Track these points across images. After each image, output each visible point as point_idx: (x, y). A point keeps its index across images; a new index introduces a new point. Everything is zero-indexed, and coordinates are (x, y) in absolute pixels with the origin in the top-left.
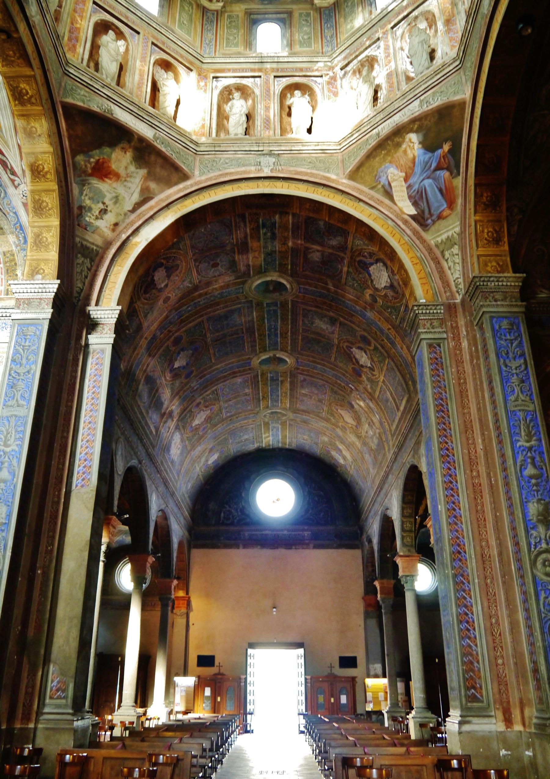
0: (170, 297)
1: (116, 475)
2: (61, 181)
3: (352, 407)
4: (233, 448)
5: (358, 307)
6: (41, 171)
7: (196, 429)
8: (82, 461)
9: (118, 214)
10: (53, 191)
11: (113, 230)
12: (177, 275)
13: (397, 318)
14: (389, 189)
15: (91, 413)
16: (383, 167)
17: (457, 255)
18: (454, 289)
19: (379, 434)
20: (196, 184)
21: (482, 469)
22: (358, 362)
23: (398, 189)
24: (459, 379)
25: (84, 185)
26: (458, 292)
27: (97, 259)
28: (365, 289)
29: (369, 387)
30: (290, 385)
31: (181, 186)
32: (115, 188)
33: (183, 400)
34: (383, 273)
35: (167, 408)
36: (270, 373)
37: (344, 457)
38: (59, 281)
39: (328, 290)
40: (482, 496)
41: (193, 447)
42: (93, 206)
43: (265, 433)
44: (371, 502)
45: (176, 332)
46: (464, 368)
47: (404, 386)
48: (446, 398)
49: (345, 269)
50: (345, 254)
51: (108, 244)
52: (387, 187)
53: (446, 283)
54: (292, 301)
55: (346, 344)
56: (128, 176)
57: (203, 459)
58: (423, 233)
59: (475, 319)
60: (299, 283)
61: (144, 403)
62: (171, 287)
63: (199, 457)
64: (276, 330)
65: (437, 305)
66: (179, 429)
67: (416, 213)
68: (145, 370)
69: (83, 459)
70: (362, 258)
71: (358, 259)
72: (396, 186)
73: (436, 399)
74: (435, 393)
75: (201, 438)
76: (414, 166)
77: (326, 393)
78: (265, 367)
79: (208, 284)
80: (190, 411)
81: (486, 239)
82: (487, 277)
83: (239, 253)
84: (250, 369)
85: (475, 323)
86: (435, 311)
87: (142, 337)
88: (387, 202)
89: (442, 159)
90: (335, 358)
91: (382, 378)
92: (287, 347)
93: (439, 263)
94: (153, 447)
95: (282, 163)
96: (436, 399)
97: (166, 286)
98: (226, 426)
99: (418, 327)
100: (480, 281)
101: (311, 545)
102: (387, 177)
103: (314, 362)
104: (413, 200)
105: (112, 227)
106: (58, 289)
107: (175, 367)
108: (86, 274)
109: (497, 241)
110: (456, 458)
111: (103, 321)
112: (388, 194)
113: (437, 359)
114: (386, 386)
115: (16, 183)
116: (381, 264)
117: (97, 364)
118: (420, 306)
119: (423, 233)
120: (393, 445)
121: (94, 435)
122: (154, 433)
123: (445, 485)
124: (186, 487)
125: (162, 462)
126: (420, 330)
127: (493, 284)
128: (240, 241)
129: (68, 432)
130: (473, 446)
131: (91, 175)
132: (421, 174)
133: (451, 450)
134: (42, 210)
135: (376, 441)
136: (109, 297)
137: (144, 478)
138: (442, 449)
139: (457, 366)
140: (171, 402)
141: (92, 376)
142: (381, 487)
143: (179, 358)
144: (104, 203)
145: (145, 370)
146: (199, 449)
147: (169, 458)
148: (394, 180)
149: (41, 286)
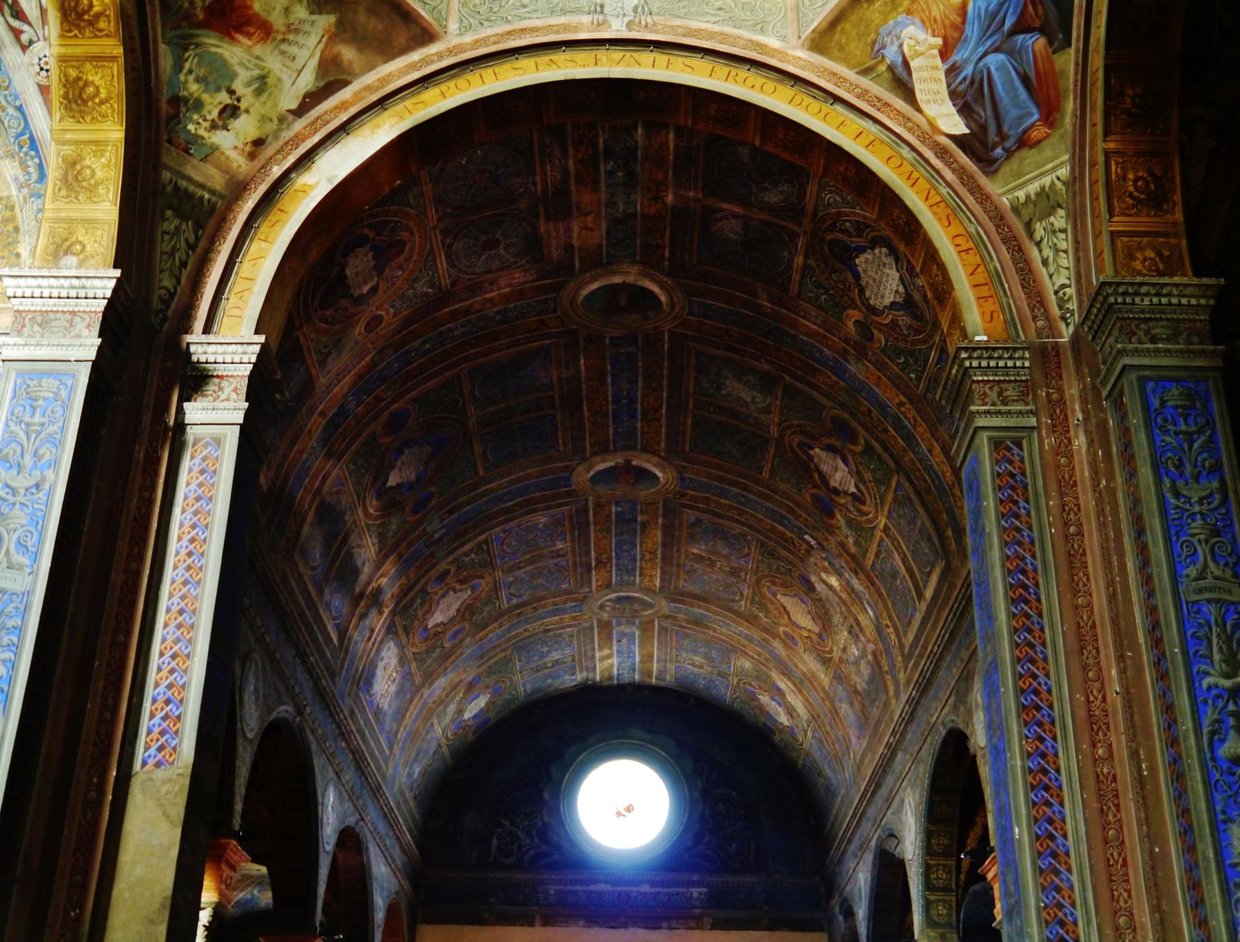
0: (381, 317)
1: (240, 740)
2: (131, 38)
3: (811, 588)
4: (524, 682)
5: (827, 352)
6: (85, 12)
7: (437, 634)
8: (159, 705)
9: (264, 119)
10: (113, 59)
11: (252, 156)
12: (400, 267)
13: (919, 379)
14: (904, 75)
15: (185, 590)
16: (891, 22)
17: (1063, 231)
18: (1056, 311)
19: (874, 653)
20: (450, 52)
21: (1119, 740)
22: (825, 480)
23: (925, 74)
24: (1066, 524)
25: (186, 49)
26: (1064, 318)
27: (213, 221)
28: (845, 309)
29: (851, 540)
30: (665, 534)
31: (415, 56)
32: (258, 58)
33: (406, 564)
34: (887, 271)
35: (369, 583)
36: (617, 504)
37: (789, 708)
38: (118, 273)
40: (1118, 807)
41: (429, 677)
42: (206, 97)
43: (601, 649)
44: (853, 817)
45: (393, 401)
46: (1077, 498)
47: (936, 541)
48: (1035, 571)
49: (799, 260)
50: (800, 225)
51: (239, 188)
52: (900, 70)
53: (1036, 297)
54: (671, 332)
55: (797, 439)
56: (292, 29)
57: (452, 708)
58: (983, 180)
59: (1104, 383)
61: (314, 569)
62: (384, 296)
63: (442, 702)
64: (633, 401)
65: (1015, 349)
66: (396, 633)
67: (967, 131)
68: (319, 490)
69: (161, 698)
70: (838, 235)
71: (829, 237)
72: (921, 69)
73: (1010, 571)
74: (1008, 557)
75: (445, 657)
76: (964, 22)
77: (748, 555)
78: (602, 489)
79: (475, 288)
80: (423, 591)
81: (1131, 196)
82: (1132, 284)
83: (548, 219)
84: (568, 494)
85: (1104, 393)
86: (1010, 363)
87: (310, 413)
88: (899, 104)
89: (1030, 8)
90: (773, 470)
91: (882, 521)
92: (659, 444)
93: (1020, 250)
94: (333, 675)
95: (654, 9)
96: (1010, 571)
97: (374, 290)
98: (509, 630)
99: (969, 400)
100: (1116, 293)
101: (708, 921)
102: (901, 46)
103: (720, 479)
104: (960, 102)
105: (248, 148)
106: (115, 291)
107: (389, 484)
108: (184, 257)
109: (1154, 200)
110: (1056, 714)
111: (220, 370)
112: (903, 85)
113: (1012, 476)
114: (893, 539)
115: (24, 38)
116: (884, 250)
117: (202, 472)
118: (974, 349)
119: (983, 180)
120: (908, 682)
121: (190, 641)
122: (335, 641)
123: (1030, 778)
124: (410, 775)
125: (352, 712)
126: (973, 408)
127: (1147, 301)
128: (551, 189)
129: (129, 633)
130: (1097, 685)
131: (205, 25)
132: (979, 43)
133: (1045, 695)
134: (85, 102)
135: (865, 670)
136: (236, 312)
137: (308, 749)
138: (1023, 691)
139: (1062, 495)
140: (378, 567)
141: (191, 500)
142: (876, 782)
143: (399, 463)
144: (231, 92)
145: (319, 490)
146: (442, 682)
147: (372, 702)
148: (918, 54)
149: (75, 282)
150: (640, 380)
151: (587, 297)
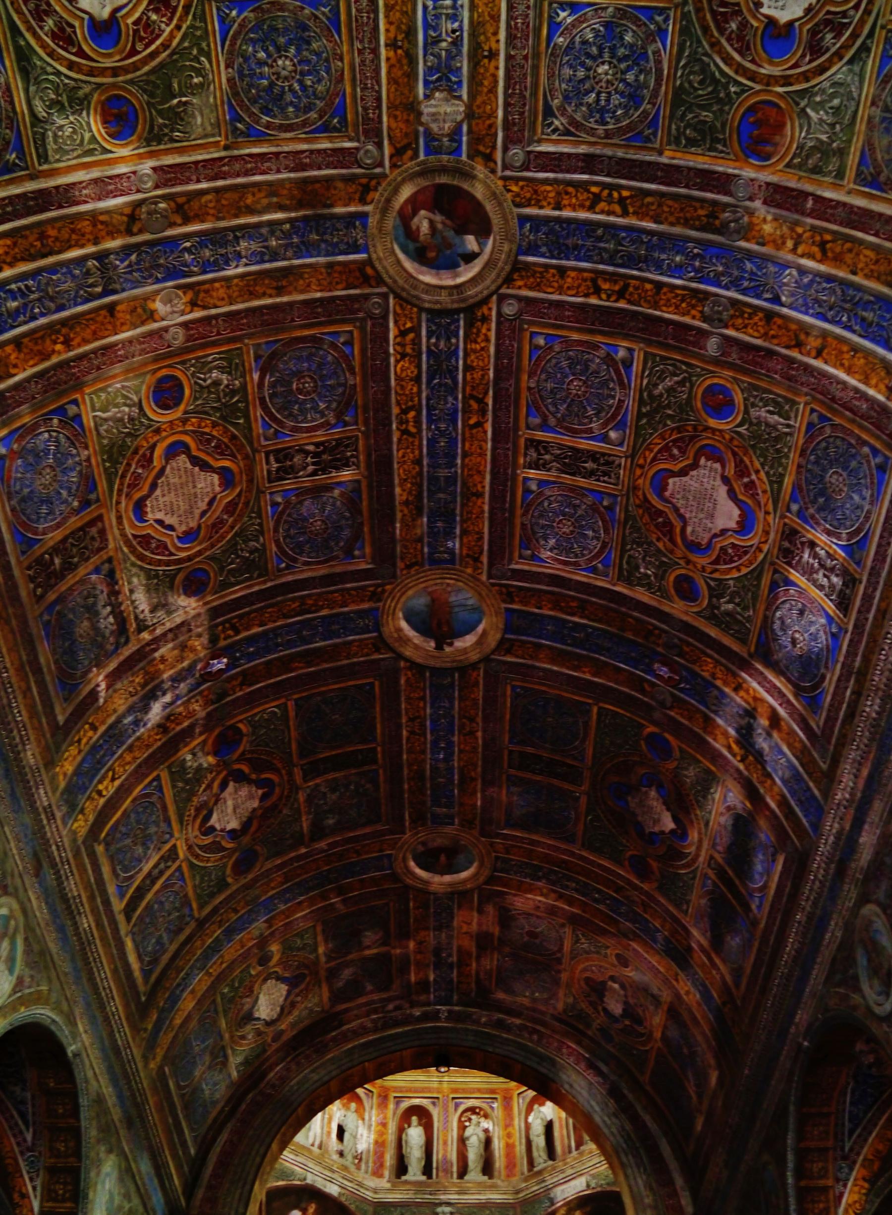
39: (340, 891)
60: (394, 877)
64: (435, 743)
79: (552, 911)
97: (612, 978)
150: (428, 773)
151: (471, 863)
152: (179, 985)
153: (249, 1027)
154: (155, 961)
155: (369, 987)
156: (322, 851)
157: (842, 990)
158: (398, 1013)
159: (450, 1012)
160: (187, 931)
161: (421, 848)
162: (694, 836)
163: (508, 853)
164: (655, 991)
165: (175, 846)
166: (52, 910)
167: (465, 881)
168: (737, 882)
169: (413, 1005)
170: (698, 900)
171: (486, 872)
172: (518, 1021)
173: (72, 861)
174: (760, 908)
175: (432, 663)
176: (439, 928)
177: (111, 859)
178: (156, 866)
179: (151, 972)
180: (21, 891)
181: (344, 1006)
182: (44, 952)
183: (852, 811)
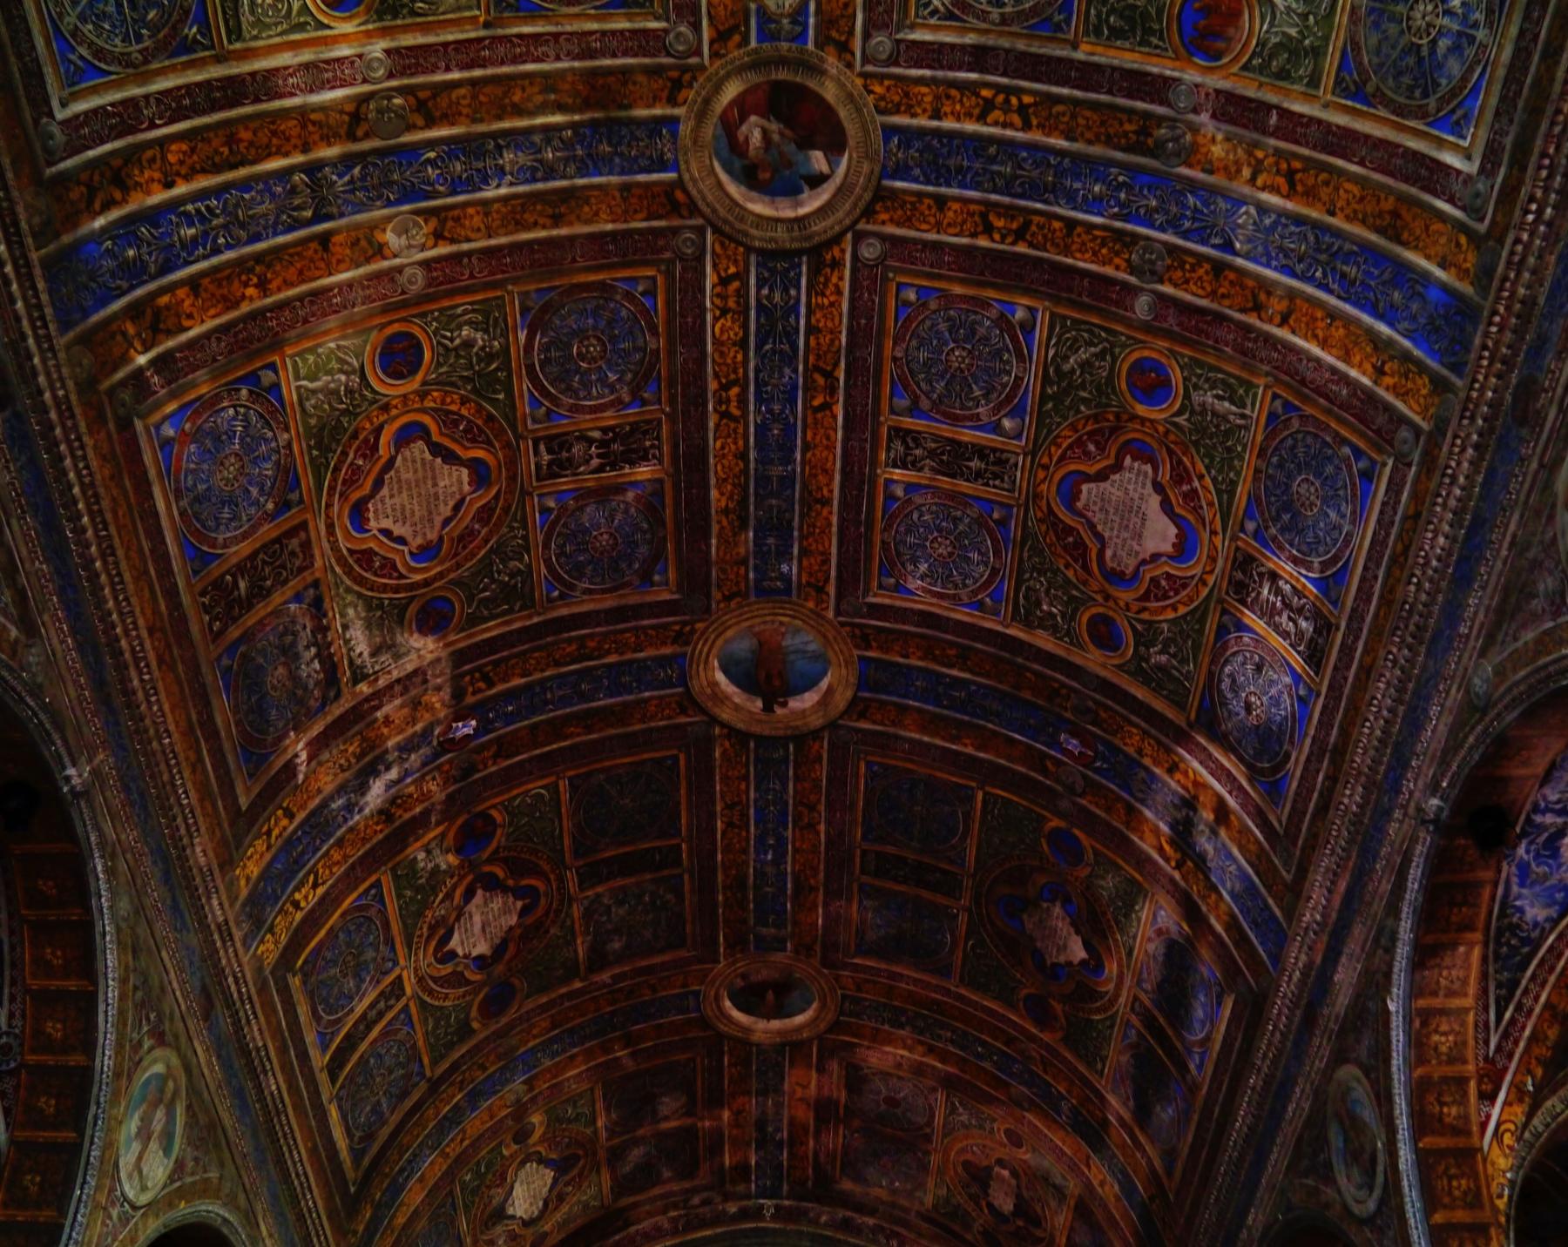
39: (628, 1040)
60: (704, 1023)
64: (761, 840)
79: (919, 1070)
83: (837, 1102)
97: (1000, 1162)
151: (809, 1004)
152: (402, 1170)
153: (499, 1229)
154: (369, 1137)
155: (667, 1174)
156: (605, 985)
157: (1310, 1182)
158: (707, 1209)
159: (777, 1207)
160: (415, 1096)
161: (739, 983)
162: (1111, 969)
163: (859, 989)
164: (1058, 1181)
165: (400, 977)
166: (226, 1065)
167: (800, 1028)
168: (1170, 1032)
169: (727, 1197)
170: (1117, 1056)
171: (830, 1017)
172: (871, 1221)
173: (255, 998)
174: (1201, 1068)
175: (756, 729)
176: (763, 1093)
177: (311, 995)
178: (372, 1006)
179: (363, 1152)
180: (183, 1039)
181: (632, 1199)
182: (214, 1125)
183: (1325, 938)
